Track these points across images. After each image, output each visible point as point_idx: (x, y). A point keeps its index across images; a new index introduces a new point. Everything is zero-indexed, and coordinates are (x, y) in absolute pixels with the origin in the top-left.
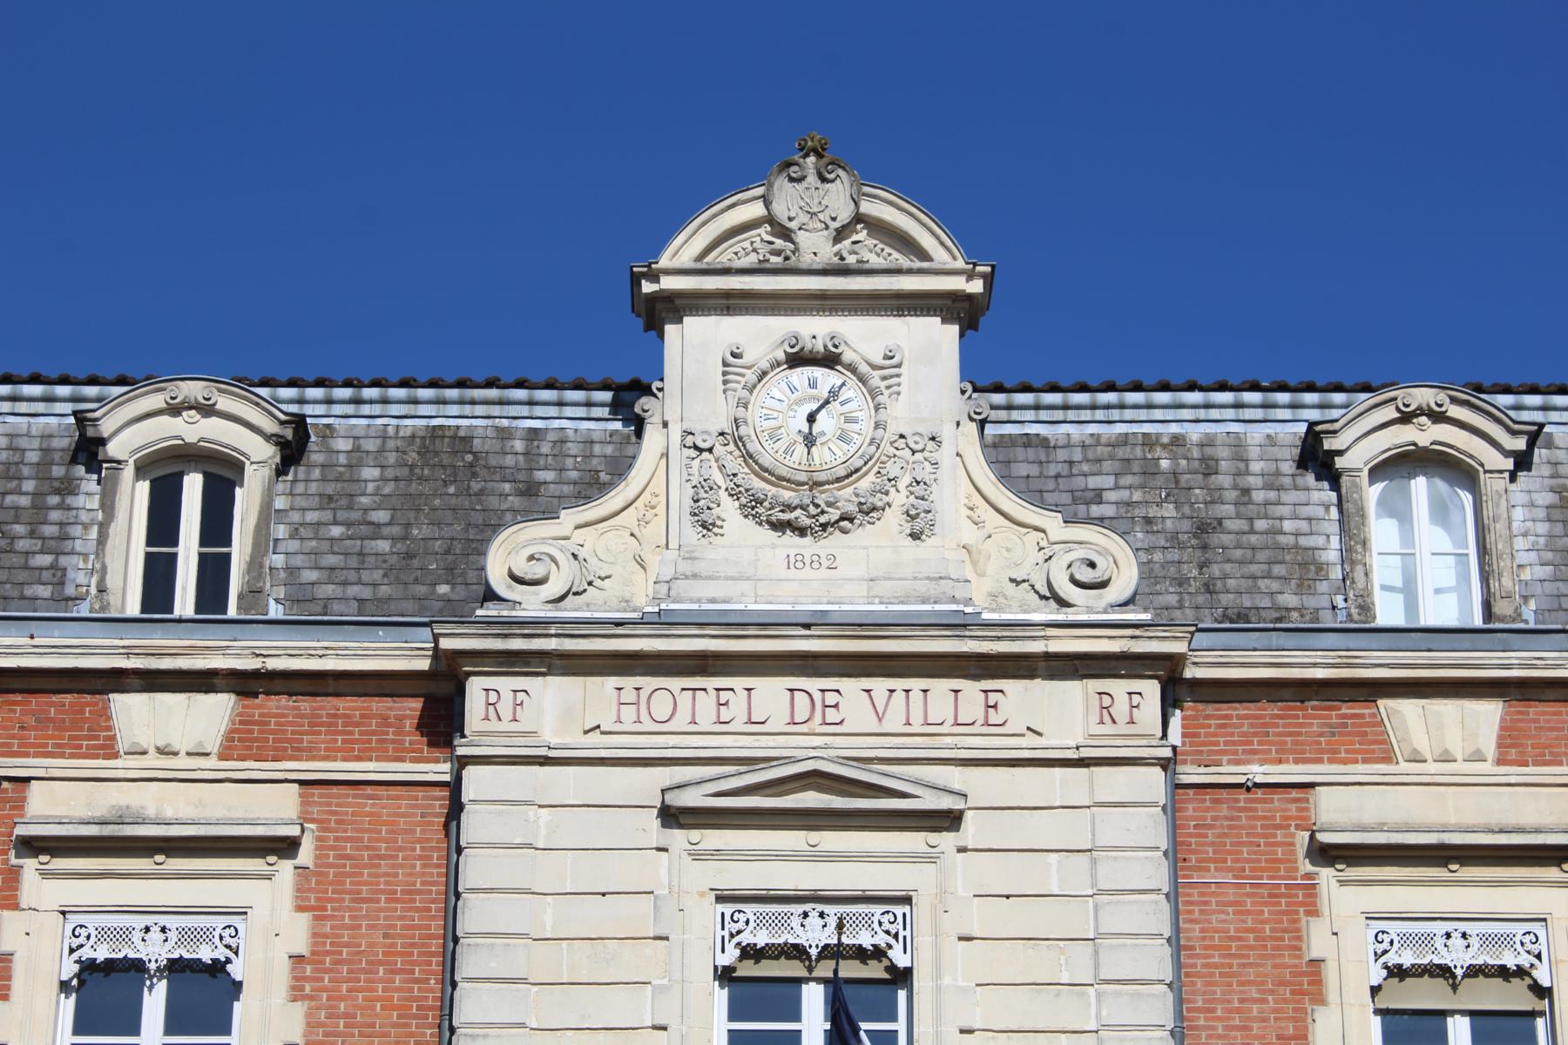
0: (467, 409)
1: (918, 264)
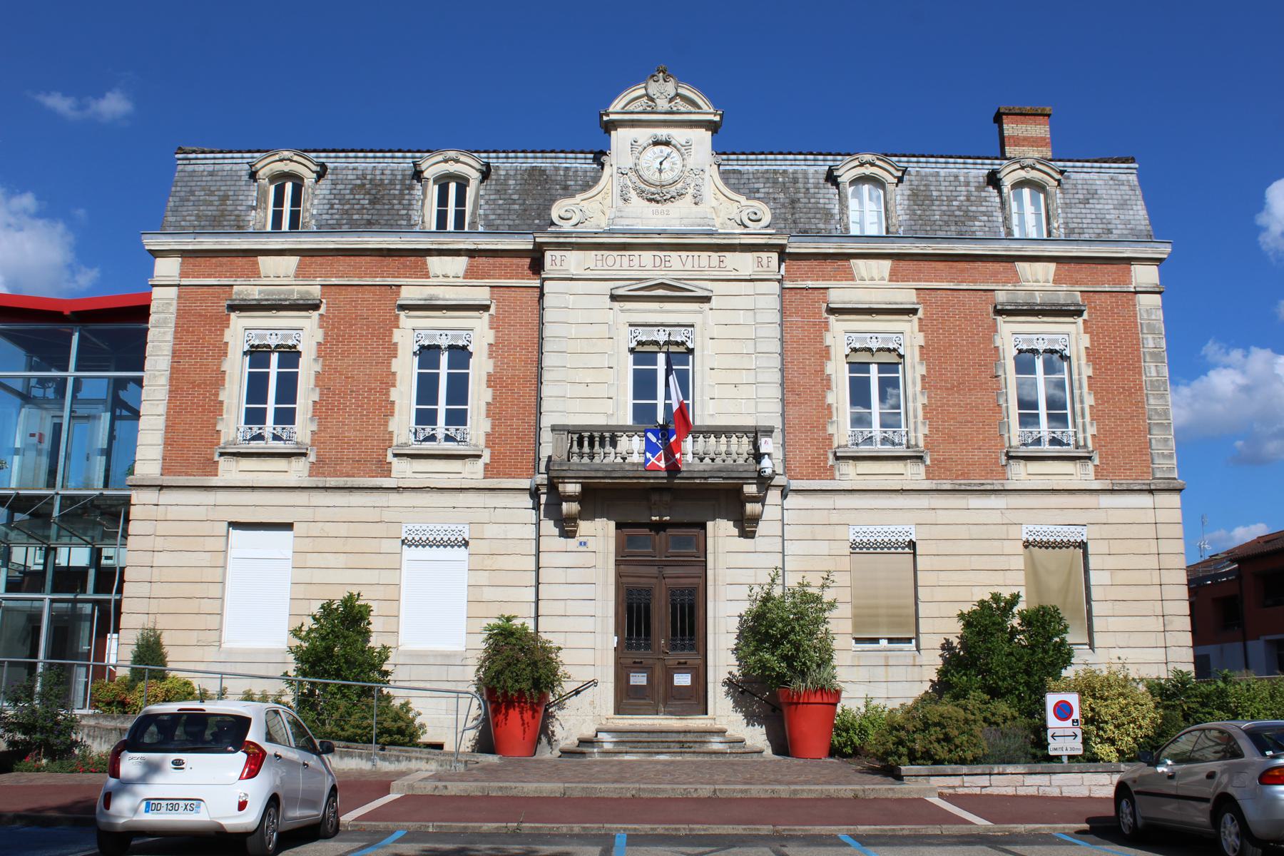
0: (544, 160)
1: (697, 111)
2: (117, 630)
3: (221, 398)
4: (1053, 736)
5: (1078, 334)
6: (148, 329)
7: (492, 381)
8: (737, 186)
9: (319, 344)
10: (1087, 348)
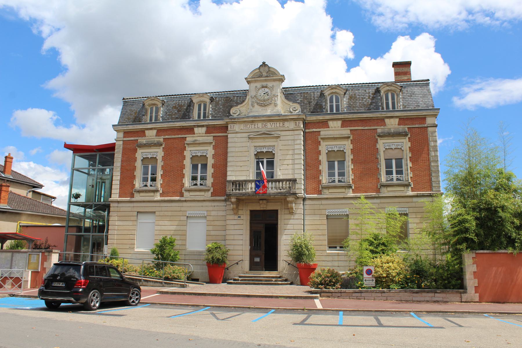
2: (107, 244)
3: (135, 174)
4: (365, 280)
5: (406, 142)
6: (114, 154)
7: (213, 166)
8: (291, 99)
9: (163, 156)
10: (409, 147)
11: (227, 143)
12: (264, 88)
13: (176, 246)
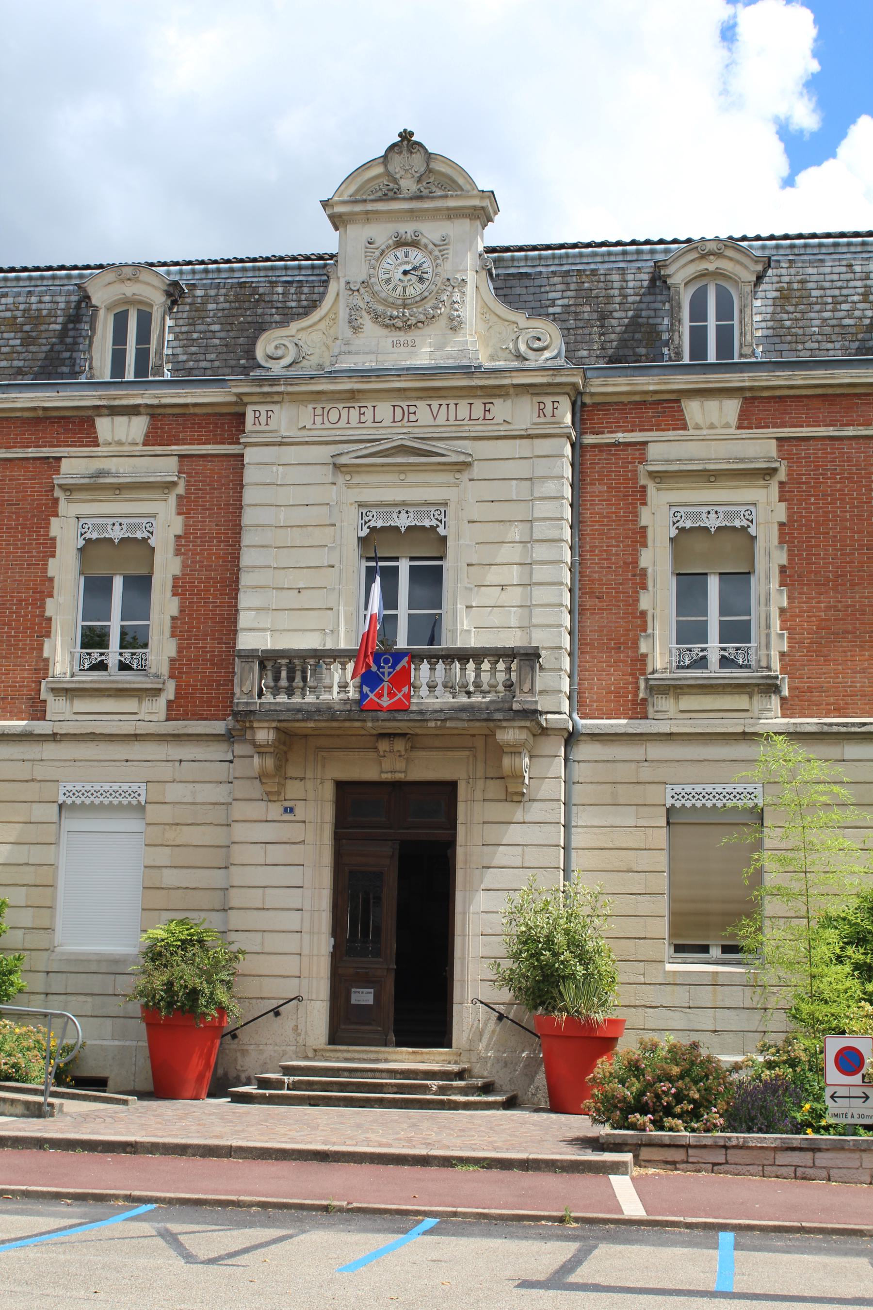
0: (257, 273)
4: (832, 1097)
7: (179, 587)
11: (239, 486)
12: (405, 249)
13: (9, 932)
